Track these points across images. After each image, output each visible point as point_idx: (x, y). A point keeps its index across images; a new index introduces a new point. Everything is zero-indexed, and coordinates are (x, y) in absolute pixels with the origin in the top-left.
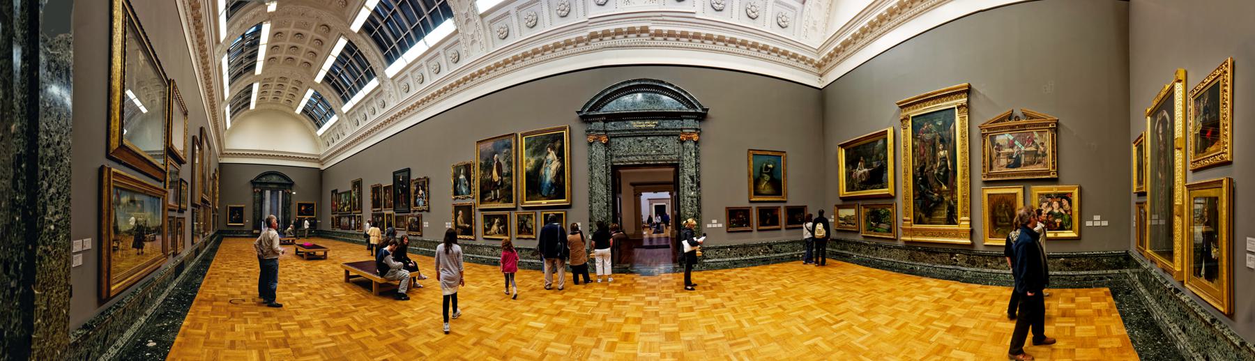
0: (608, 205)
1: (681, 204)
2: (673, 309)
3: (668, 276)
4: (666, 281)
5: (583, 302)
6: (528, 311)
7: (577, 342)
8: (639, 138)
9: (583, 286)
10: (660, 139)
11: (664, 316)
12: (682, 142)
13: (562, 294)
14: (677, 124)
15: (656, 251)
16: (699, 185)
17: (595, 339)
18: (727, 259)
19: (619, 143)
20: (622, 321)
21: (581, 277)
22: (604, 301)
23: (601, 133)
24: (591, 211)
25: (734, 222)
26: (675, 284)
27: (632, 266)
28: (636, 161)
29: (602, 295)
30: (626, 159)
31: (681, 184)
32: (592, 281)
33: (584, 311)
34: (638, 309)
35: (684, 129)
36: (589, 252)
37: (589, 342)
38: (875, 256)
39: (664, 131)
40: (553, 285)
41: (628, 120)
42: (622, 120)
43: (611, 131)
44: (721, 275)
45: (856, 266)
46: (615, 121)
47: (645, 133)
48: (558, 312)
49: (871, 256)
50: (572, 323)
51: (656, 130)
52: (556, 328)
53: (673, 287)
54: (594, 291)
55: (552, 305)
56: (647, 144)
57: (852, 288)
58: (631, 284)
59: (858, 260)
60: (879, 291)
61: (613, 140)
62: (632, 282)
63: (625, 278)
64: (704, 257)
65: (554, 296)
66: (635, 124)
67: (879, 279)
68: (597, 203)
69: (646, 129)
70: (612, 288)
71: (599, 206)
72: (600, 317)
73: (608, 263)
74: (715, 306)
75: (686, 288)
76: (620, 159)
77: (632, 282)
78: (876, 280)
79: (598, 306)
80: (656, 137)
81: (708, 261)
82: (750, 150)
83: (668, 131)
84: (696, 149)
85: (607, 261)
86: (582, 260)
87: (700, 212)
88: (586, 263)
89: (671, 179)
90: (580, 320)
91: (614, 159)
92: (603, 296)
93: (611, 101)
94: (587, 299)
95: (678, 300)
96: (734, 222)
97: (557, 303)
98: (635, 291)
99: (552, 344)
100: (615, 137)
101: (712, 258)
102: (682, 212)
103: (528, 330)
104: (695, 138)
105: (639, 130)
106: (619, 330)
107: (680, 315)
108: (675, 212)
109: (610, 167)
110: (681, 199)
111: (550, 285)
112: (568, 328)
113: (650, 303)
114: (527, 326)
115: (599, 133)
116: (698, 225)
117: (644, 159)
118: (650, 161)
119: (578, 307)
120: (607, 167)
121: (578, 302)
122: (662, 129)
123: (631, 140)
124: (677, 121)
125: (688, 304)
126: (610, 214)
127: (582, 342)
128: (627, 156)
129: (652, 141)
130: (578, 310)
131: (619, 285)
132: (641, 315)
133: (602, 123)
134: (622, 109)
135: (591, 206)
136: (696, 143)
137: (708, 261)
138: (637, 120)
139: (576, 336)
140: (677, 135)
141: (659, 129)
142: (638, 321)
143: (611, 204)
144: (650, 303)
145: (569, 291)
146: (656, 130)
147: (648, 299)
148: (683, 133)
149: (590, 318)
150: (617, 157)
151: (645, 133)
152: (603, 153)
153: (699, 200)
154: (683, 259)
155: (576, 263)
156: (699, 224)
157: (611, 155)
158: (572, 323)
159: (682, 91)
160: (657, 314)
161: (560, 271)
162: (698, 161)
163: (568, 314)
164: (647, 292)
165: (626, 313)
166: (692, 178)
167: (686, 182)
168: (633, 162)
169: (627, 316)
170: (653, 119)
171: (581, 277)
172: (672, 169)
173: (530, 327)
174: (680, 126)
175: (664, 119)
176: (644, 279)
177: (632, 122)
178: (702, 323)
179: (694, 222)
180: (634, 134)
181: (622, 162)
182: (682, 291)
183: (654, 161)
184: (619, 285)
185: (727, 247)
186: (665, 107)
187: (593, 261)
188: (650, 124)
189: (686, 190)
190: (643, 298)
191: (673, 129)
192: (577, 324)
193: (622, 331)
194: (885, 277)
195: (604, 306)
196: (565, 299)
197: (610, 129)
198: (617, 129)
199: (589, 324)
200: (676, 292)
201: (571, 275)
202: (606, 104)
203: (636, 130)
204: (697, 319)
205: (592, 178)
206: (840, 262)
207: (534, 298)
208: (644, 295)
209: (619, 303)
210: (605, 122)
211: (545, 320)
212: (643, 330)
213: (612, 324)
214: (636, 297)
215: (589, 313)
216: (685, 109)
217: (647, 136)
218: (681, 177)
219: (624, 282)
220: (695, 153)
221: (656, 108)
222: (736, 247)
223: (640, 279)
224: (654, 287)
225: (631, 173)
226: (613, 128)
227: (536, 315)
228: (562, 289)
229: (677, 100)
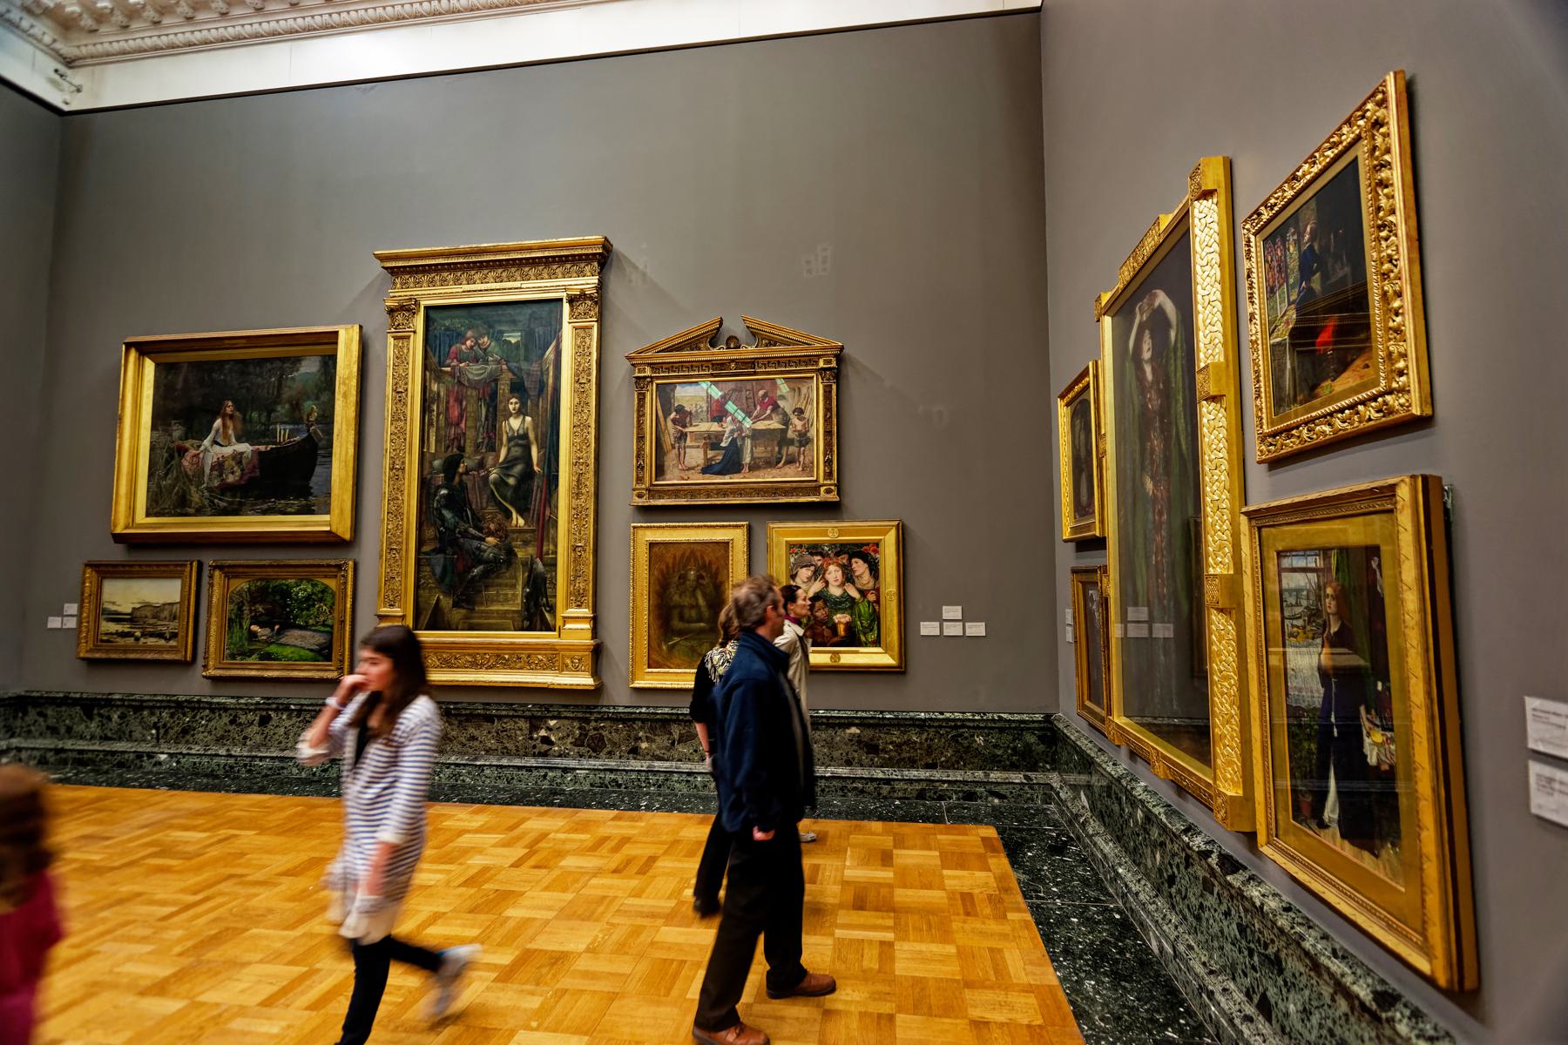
38: (258, 747)
45: (162, 795)
49: (236, 751)
57: (126, 889)
59: (174, 773)
60: (259, 876)
67: (262, 830)
78: (248, 837)
194: (289, 819)
206: (91, 792)
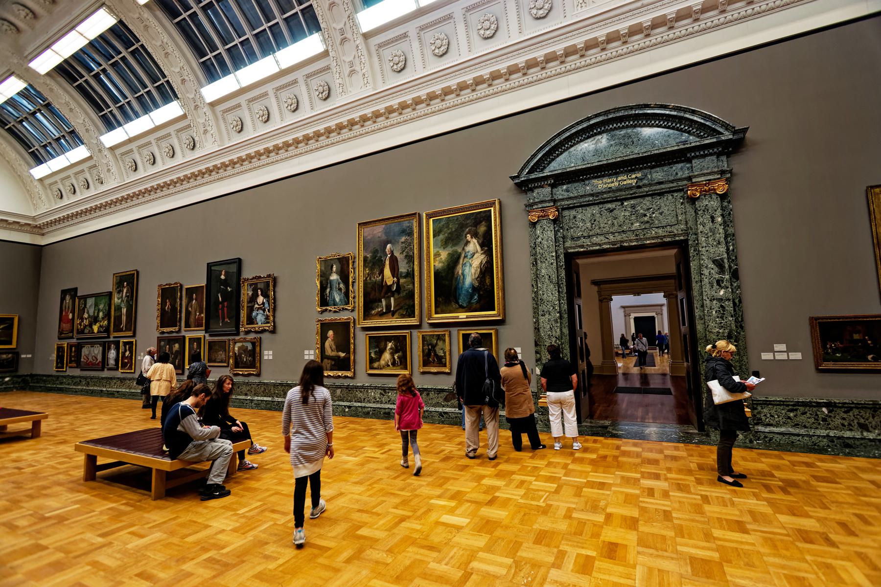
0: (561, 317)
1: (697, 313)
2: (698, 518)
3: (676, 449)
4: (674, 458)
5: (531, 483)
6: (439, 497)
7: (522, 554)
8: (609, 206)
9: (530, 454)
10: (647, 202)
11: (683, 523)
12: (693, 200)
13: (495, 466)
14: (680, 170)
15: (651, 398)
16: (735, 275)
17: (555, 550)
18: (823, 432)
19: (575, 217)
20: (600, 518)
21: (525, 439)
22: (567, 484)
23: (548, 204)
24: (537, 329)
25: (835, 351)
26: (693, 466)
27: (614, 424)
28: (605, 243)
29: (564, 471)
30: (587, 242)
31: (694, 276)
32: (544, 447)
33: (533, 499)
34: (629, 500)
35: (695, 176)
36: (536, 396)
37: (543, 555)
39: (654, 188)
40: (479, 451)
41: (589, 179)
42: (579, 181)
43: (563, 200)
44: (808, 465)
46: (568, 183)
47: (618, 197)
48: (489, 498)
50: (513, 519)
51: (639, 187)
52: (487, 526)
53: (690, 472)
54: (549, 464)
55: (479, 484)
56: (622, 213)
58: (616, 458)
61: (566, 213)
62: (616, 453)
63: (604, 446)
64: (759, 422)
65: (482, 471)
66: (601, 184)
68: (547, 316)
69: (619, 189)
70: (581, 461)
71: (549, 320)
72: (562, 512)
73: (571, 416)
74: (805, 536)
75: (720, 480)
76: (579, 243)
77: (616, 453)
79: (557, 491)
80: (638, 200)
81: (767, 430)
82: (872, 187)
83: (663, 186)
84: (723, 209)
85: (569, 412)
86: (526, 410)
87: (742, 327)
88: (532, 415)
89: (672, 269)
90: (527, 513)
91: (568, 244)
92: (566, 475)
93: (562, 153)
94: (538, 478)
95: (706, 499)
96: (835, 351)
97: (486, 481)
98: (620, 466)
99: (481, 555)
100: (569, 208)
101: (777, 425)
102: (699, 327)
103: (440, 529)
104: (721, 188)
105: (609, 192)
106: (596, 535)
107: (717, 533)
108: (684, 329)
109: (562, 256)
110: (697, 304)
111: (475, 450)
112: (507, 527)
113: (651, 492)
114: (438, 523)
115: (544, 205)
116: (738, 353)
117: (619, 238)
118: (631, 241)
119: (522, 492)
120: (557, 257)
121: (522, 483)
122: (650, 185)
123: (595, 210)
124: (680, 165)
125: (732, 513)
126: (566, 331)
127: (531, 556)
128: (589, 237)
129: (633, 207)
130: (522, 497)
131: (594, 456)
132: (635, 513)
133: (549, 189)
134: (579, 163)
135: (537, 322)
136: (723, 197)
137: (767, 430)
138: (603, 176)
139: (521, 544)
140: (682, 190)
141: (645, 185)
142: (632, 523)
143: (566, 316)
144: (651, 492)
145: (507, 461)
146: (639, 187)
147: (647, 483)
148: (693, 184)
149: (545, 511)
150: (573, 239)
151: (618, 197)
152: (551, 234)
153: (738, 304)
154: (713, 418)
155: (517, 414)
156: (742, 351)
157: (564, 237)
158: (513, 519)
159: (686, 110)
160: (667, 515)
161: (490, 426)
162: (731, 230)
163: (505, 503)
164: (642, 470)
165: (606, 506)
166: (719, 264)
167: (706, 272)
168: (600, 245)
169: (609, 510)
170: (633, 171)
171: (525, 439)
172: (673, 252)
173: (444, 524)
174: (686, 174)
175: (652, 167)
176: (635, 445)
177: (595, 181)
178: (774, 565)
179: (732, 347)
180: (599, 200)
181: (582, 246)
182: (711, 483)
183: (637, 240)
184: (594, 456)
185: (819, 405)
186: (653, 145)
187: (545, 411)
188: (628, 180)
189: (706, 288)
190: (637, 480)
191: (672, 182)
192: (522, 522)
193: (602, 538)
195: (567, 491)
196: (499, 475)
197: (561, 197)
198: (572, 195)
199: (543, 523)
200: (699, 482)
201: (509, 433)
202: (553, 160)
203: (602, 193)
204: (758, 552)
205: (537, 277)
207: (449, 473)
208: (638, 476)
209: (592, 485)
210: (553, 186)
211: (469, 511)
212: (642, 542)
213: (582, 523)
214: (623, 477)
215: (541, 503)
216: (693, 141)
217: (622, 201)
218: (693, 265)
219: (602, 452)
220: (722, 215)
221: (637, 151)
222: (848, 408)
223: (628, 446)
224: (655, 462)
225: (599, 263)
226: (566, 195)
227: (453, 504)
228: (495, 458)
229: (677, 129)
